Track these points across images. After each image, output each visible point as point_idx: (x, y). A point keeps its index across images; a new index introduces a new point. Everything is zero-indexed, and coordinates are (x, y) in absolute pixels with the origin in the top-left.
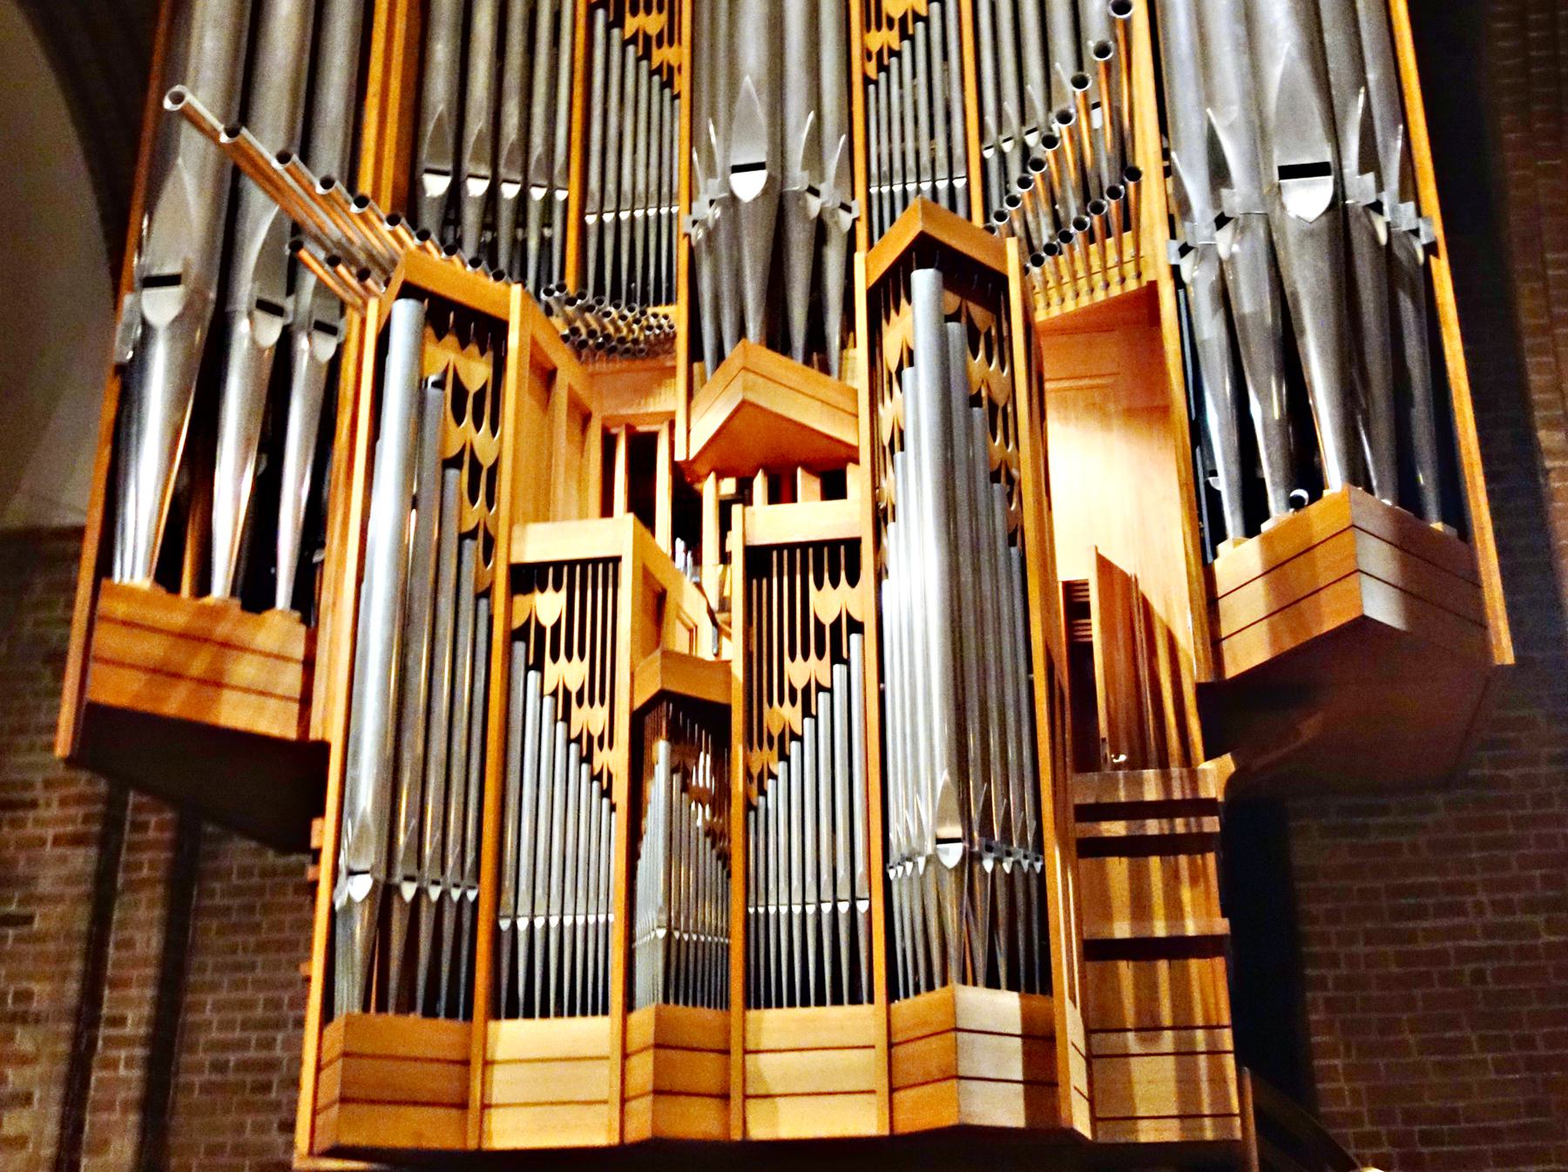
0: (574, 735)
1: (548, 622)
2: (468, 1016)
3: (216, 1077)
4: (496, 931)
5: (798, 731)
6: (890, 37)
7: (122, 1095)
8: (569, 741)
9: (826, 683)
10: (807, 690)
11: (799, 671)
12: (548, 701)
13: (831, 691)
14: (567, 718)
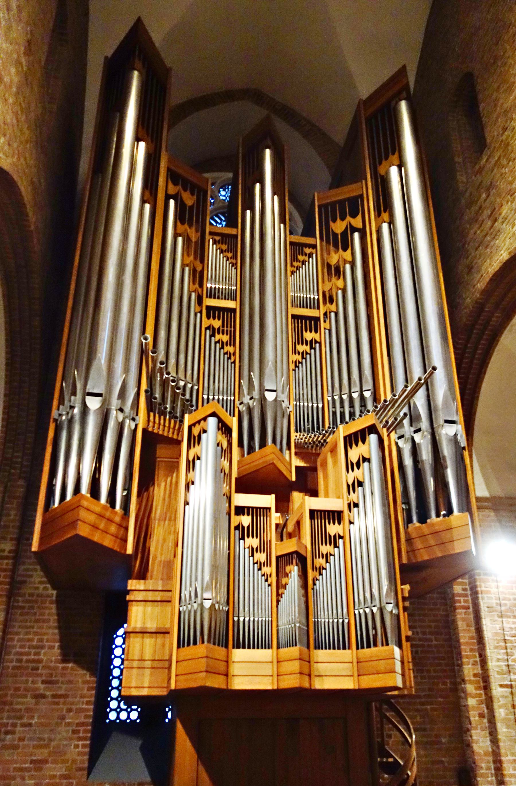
0: (255, 561)
2: (227, 647)
3: (18, 664)
4: (234, 620)
5: (325, 567)
6: (299, 358)
8: (254, 564)
9: (333, 553)
10: (327, 555)
11: (325, 549)
13: (334, 555)
14: (253, 555)
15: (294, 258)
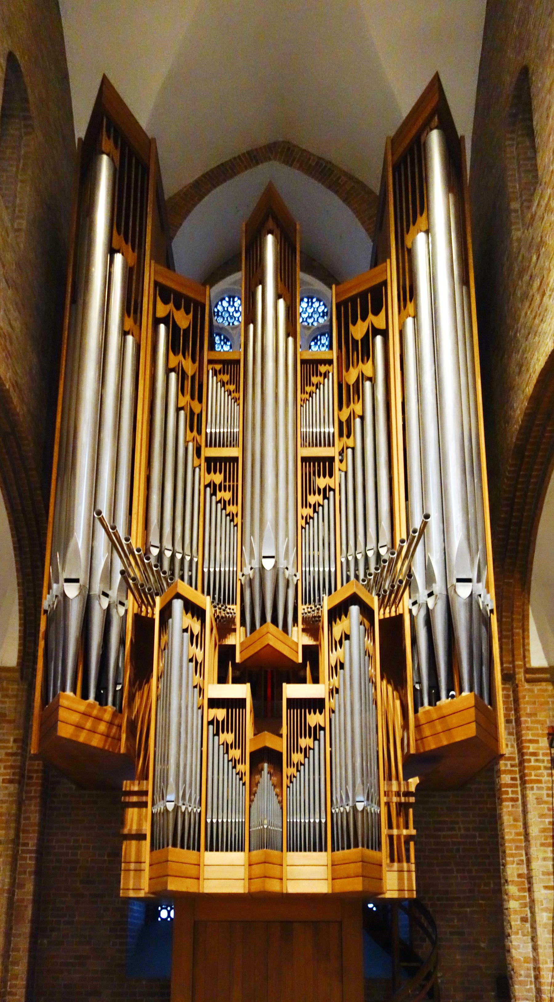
0: (230, 758)
1: (220, 719)
7: (28, 870)
8: (228, 761)
12: (221, 747)
14: (227, 752)
15: (306, 381)
